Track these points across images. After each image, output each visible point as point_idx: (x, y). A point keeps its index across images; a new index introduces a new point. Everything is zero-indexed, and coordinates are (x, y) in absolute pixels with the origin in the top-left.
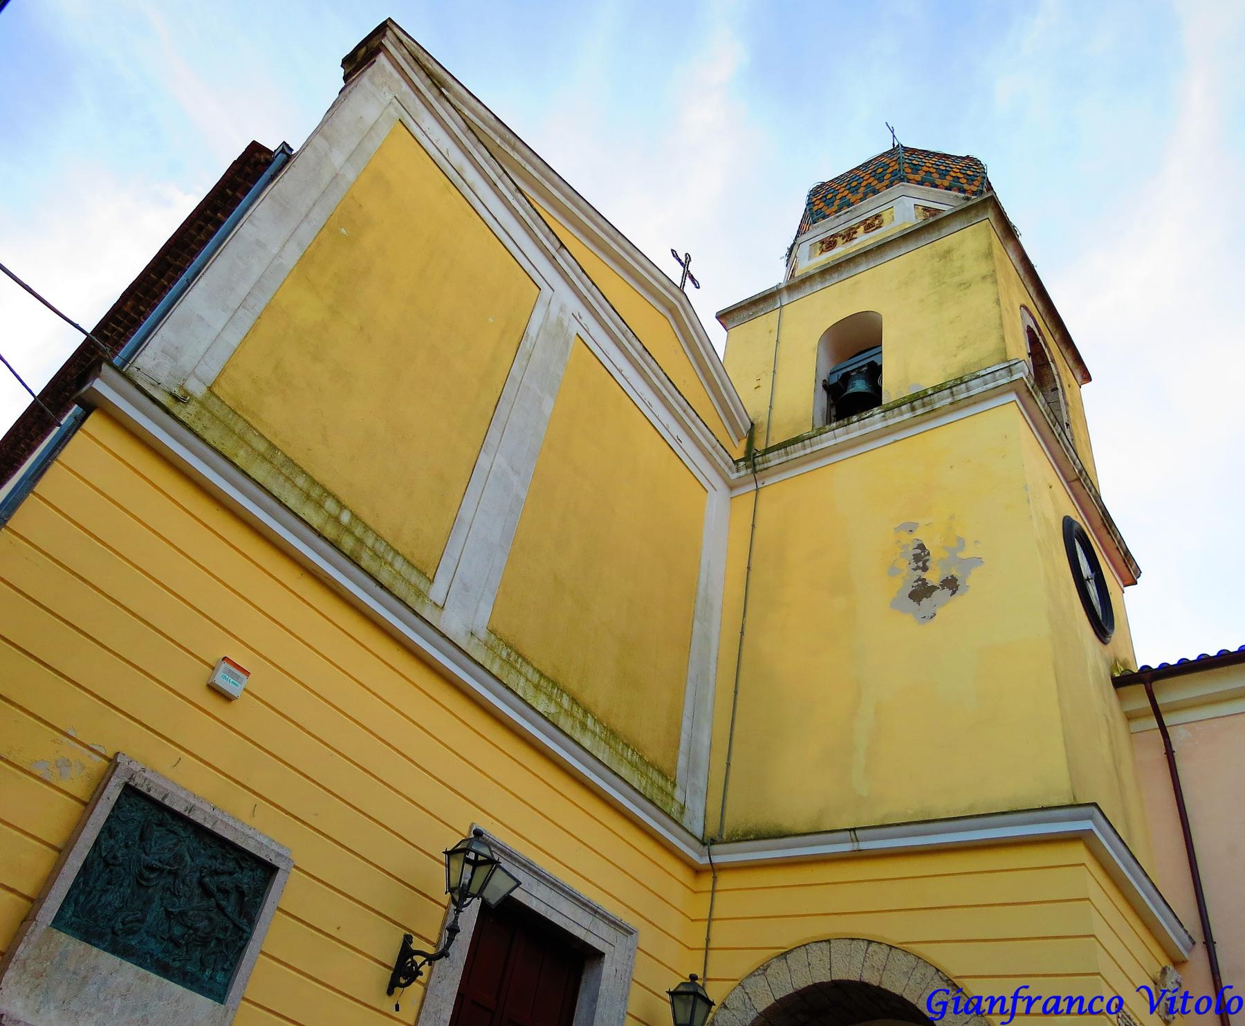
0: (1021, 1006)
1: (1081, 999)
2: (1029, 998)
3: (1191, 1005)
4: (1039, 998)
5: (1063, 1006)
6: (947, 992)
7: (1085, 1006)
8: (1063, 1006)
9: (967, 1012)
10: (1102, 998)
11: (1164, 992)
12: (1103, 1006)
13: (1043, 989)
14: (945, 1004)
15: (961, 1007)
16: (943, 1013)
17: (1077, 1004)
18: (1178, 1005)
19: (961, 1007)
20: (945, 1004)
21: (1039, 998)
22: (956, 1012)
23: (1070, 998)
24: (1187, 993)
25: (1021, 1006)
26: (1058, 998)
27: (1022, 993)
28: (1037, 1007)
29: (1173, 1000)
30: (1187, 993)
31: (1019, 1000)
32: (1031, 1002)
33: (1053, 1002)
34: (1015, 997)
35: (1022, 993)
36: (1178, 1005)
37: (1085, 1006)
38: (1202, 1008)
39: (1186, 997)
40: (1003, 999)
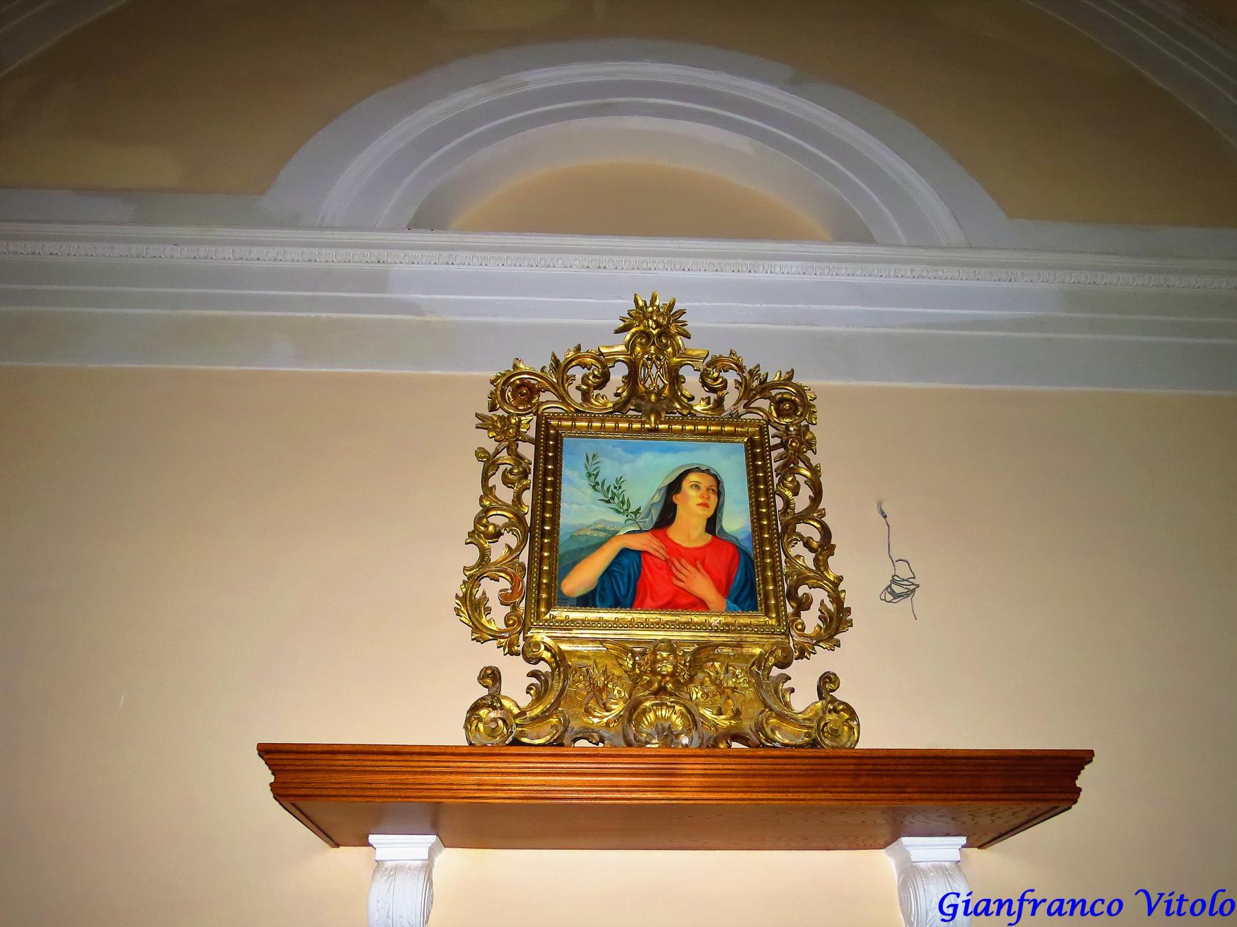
0: (1028, 908)
1: (1084, 901)
2: (1035, 901)
3: (1186, 907)
4: (1044, 901)
5: (1067, 908)
6: (958, 895)
7: (1087, 909)
8: (1067, 908)
9: (977, 914)
10: (1103, 901)
11: (1161, 895)
12: (1104, 908)
13: (1047, 891)
14: (955, 907)
15: (971, 909)
16: (954, 915)
17: (1006, 907)
18: (1174, 907)
19: (971, 909)
20: (955, 907)
21: (1044, 901)
22: (966, 913)
23: (1073, 901)
24: (1182, 896)
25: (1028, 908)
26: (988, 901)
27: (1029, 896)
28: (1043, 908)
29: (1169, 902)
30: (1182, 896)
31: (1025, 903)
32: (1036, 905)
33: (1057, 904)
34: (1022, 900)
35: (1029, 896)
36: (1174, 907)
37: (1087, 909)
38: (1197, 910)
39: (1181, 900)
40: (1010, 901)
